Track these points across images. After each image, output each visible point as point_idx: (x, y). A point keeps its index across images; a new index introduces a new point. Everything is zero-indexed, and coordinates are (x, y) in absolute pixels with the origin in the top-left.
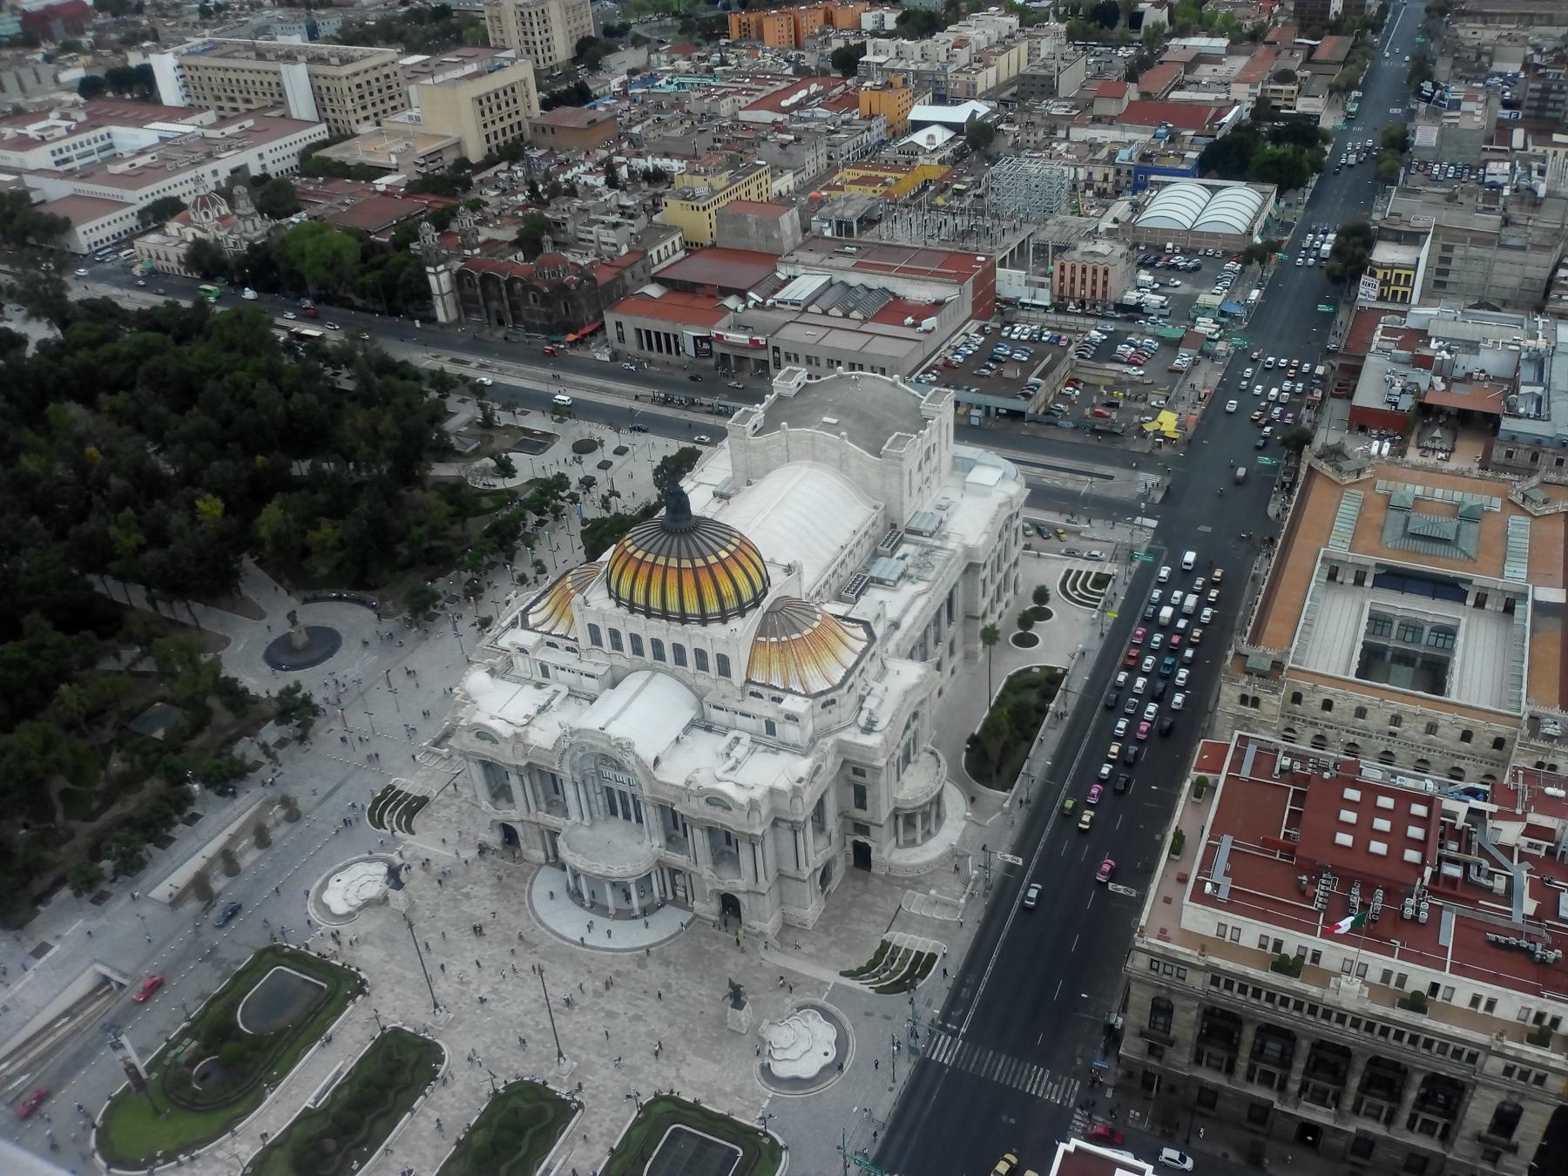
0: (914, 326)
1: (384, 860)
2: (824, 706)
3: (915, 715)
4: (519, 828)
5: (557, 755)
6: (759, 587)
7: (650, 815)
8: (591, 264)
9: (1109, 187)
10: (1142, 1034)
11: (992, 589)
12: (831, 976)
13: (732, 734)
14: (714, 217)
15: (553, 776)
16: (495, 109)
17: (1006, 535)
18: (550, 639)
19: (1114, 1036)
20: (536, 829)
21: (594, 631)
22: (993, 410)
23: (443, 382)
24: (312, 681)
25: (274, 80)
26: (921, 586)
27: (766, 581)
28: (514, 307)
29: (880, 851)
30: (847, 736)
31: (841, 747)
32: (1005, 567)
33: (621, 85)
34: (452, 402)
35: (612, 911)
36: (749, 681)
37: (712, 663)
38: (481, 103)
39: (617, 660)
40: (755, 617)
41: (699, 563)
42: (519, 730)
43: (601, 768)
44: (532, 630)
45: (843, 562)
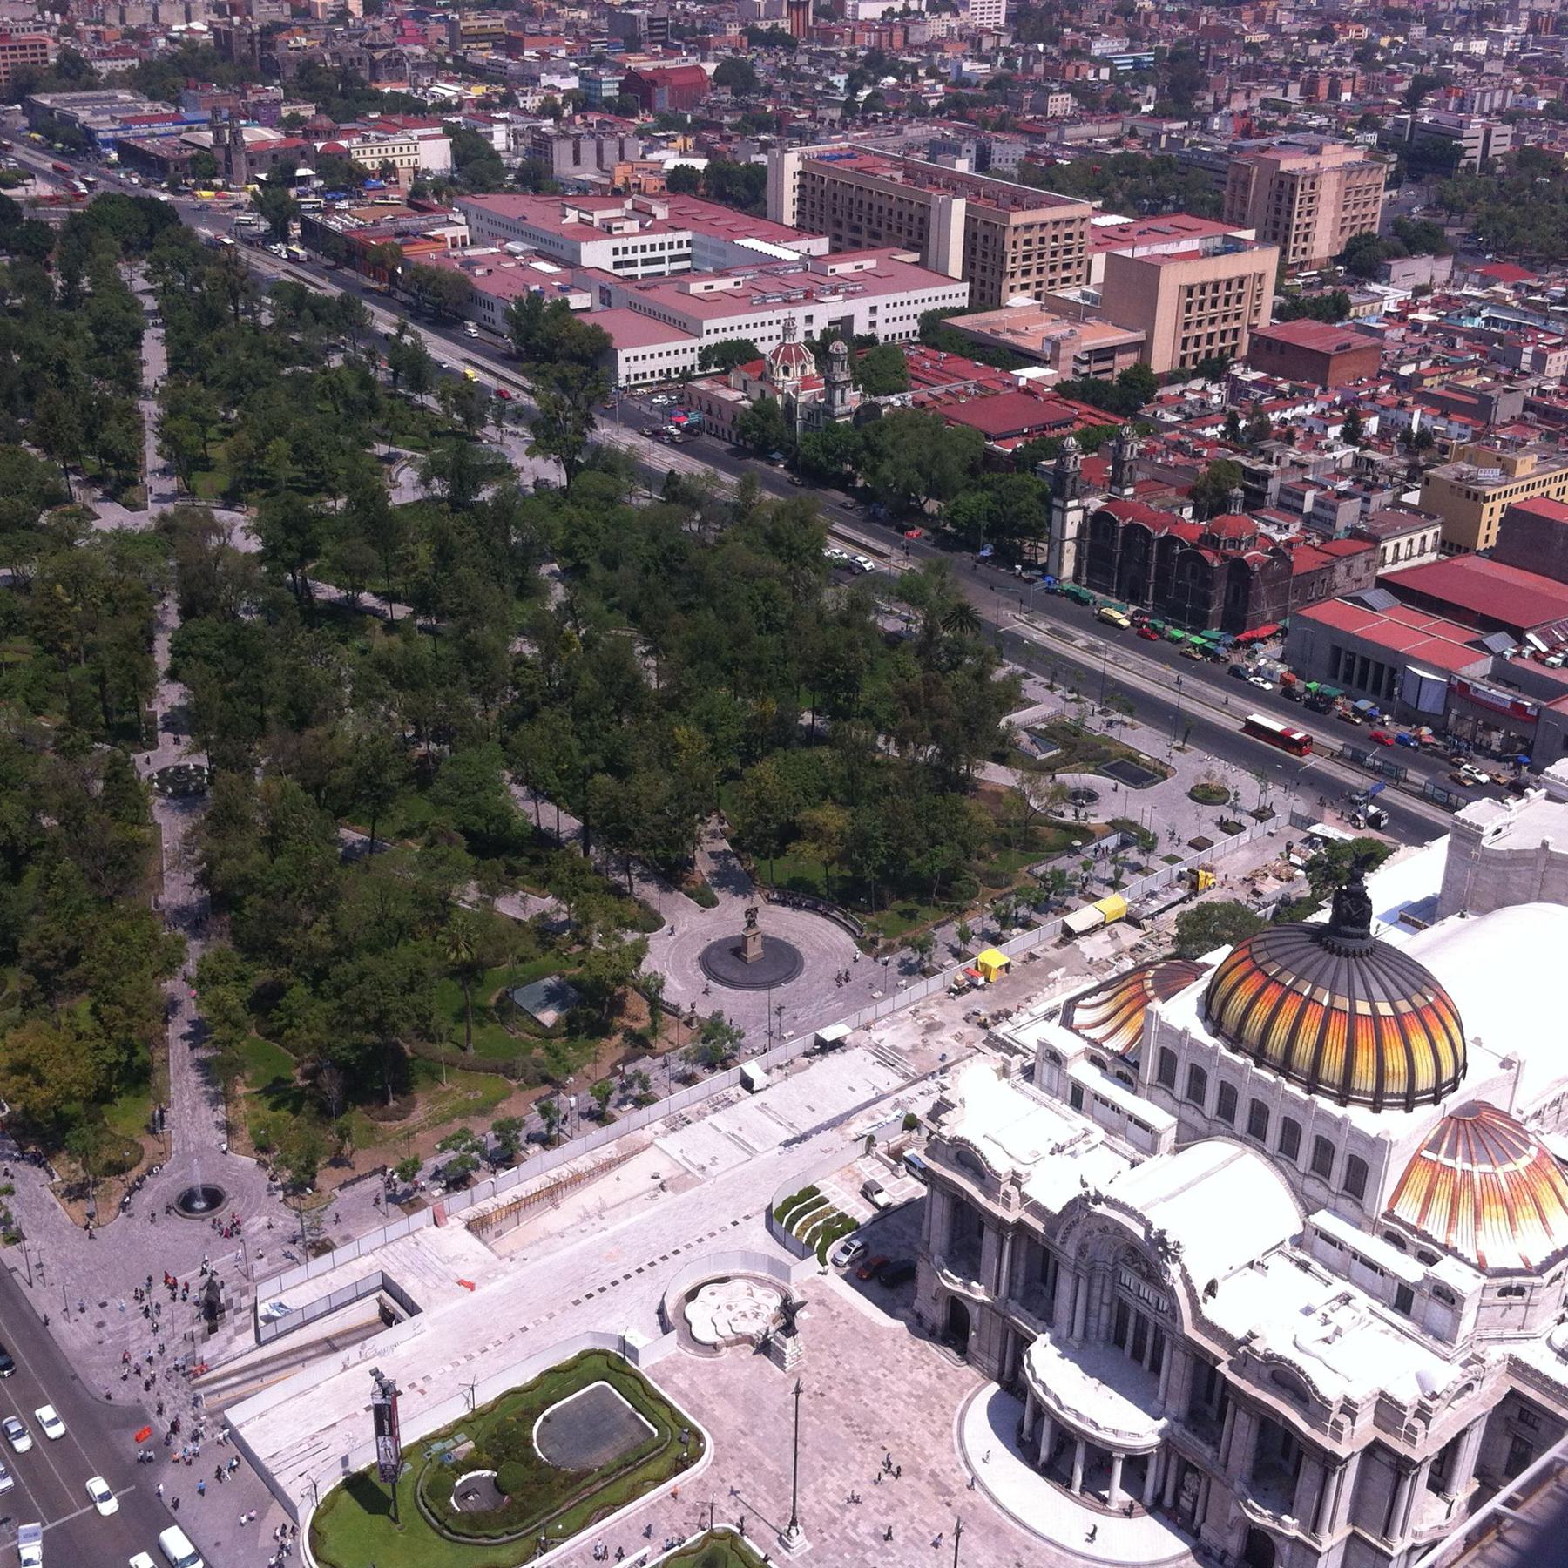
1: (777, 1287)
2: (1505, 1292)
4: (975, 1313)
6: (1448, 1072)
8: (1289, 543)
14: (1498, 515)
20: (998, 1323)
21: (1167, 1061)
27: (1461, 1068)
28: (1162, 576)
31: (1517, 1367)
33: (1400, 304)
34: (1033, 687)
36: (1389, 1215)
37: (1339, 1168)
38: (1190, 294)
39: (1189, 1114)
40: (1427, 1117)
41: (1363, 1008)
42: (1020, 1169)
43: (1122, 1268)
44: (1076, 1031)
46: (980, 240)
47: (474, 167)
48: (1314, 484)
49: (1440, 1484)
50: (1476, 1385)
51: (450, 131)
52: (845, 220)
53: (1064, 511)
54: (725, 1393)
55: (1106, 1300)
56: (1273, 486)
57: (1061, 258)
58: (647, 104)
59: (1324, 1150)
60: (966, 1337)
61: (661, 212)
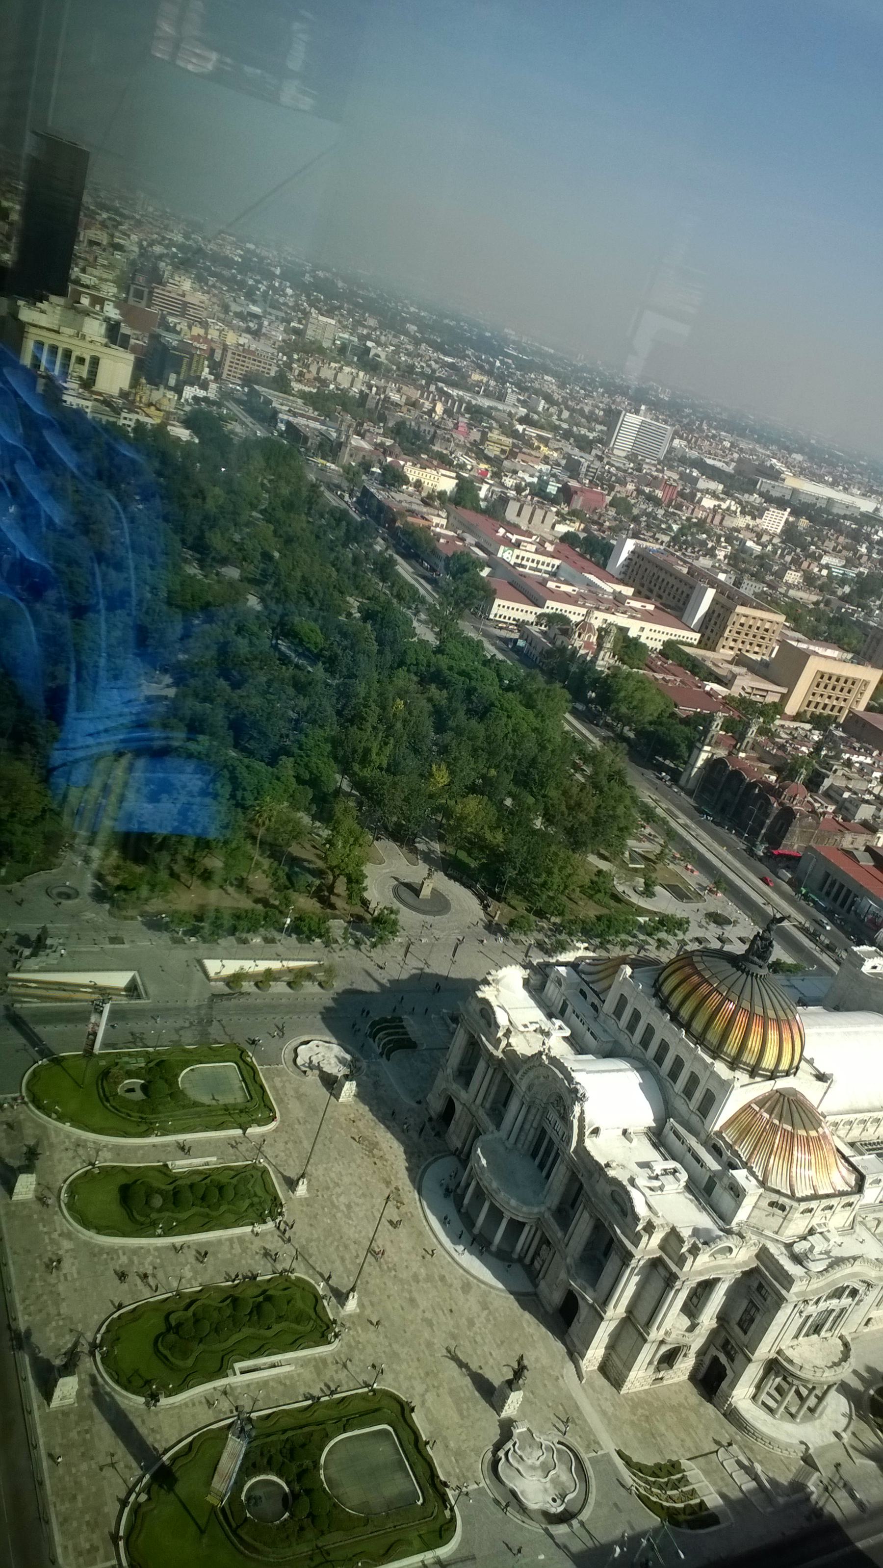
2: (772, 1204)
3: (854, 1293)
4: (458, 1107)
5: (526, 1067)
6: (784, 1065)
7: (559, 1175)
12: (609, 1446)
13: (672, 1164)
15: (512, 1086)
16: (830, 687)
23: (649, 816)
24: (407, 917)
25: (686, 589)
29: (733, 1386)
30: (773, 1249)
31: (763, 1254)
35: (476, 1231)
36: (719, 1134)
37: (698, 1095)
38: (822, 678)
43: (550, 1108)
44: (578, 973)
46: (716, 615)
47: (464, 494)
48: (849, 790)
49: (692, 1309)
50: (735, 1251)
51: (458, 477)
52: (646, 584)
53: (700, 750)
54: (300, 1097)
55: (535, 1125)
56: (827, 783)
57: (758, 640)
58: (568, 502)
59: (694, 1080)
60: (448, 1125)
61: (550, 548)
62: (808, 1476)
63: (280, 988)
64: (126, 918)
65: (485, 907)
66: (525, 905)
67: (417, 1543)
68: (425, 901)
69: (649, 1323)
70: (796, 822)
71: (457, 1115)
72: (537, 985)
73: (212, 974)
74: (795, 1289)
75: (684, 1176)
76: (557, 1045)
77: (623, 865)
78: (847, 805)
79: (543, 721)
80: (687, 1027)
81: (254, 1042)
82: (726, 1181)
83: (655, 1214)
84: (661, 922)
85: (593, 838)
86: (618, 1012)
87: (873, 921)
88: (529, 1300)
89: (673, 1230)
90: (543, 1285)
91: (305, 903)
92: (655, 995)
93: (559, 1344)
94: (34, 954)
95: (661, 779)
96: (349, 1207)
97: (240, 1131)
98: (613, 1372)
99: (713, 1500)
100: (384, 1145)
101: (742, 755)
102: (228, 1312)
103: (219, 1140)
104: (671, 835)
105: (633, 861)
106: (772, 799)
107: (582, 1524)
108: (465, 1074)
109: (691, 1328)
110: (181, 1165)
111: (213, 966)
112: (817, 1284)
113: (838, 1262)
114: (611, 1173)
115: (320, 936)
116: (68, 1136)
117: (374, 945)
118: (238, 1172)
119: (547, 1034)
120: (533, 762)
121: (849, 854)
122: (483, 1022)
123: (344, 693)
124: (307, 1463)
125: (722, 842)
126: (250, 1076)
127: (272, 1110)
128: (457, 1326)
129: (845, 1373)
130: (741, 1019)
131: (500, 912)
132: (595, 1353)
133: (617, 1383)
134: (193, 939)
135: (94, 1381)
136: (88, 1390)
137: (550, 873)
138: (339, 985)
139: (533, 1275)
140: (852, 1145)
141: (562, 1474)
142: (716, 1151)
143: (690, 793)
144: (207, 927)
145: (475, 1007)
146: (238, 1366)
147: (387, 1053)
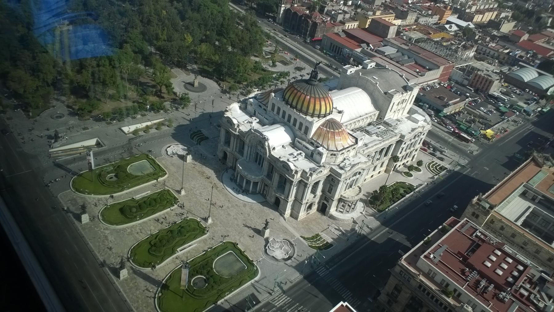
0: (417, 73)
2: (331, 155)
3: (360, 173)
4: (228, 154)
6: (328, 112)
9: (504, 61)
10: (388, 295)
11: (404, 153)
12: (298, 235)
17: (417, 138)
18: (260, 104)
19: (379, 293)
22: (432, 107)
23: (268, 37)
24: (192, 95)
26: (380, 138)
29: (330, 209)
30: (334, 167)
31: (332, 170)
32: (412, 149)
35: (243, 189)
36: (312, 139)
37: (303, 128)
40: (323, 120)
45: (359, 121)
48: (334, 10)
49: (314, 191)
53: (281, 7)
54: (173, 165)
56: (326, 9)
59: (301, 124)
62: (355, 226)
63: (153, 131)
64: (86, 120)
65: (219, 85)
66: (233, 80)
67: (248, 279)
68: (196, 88)
69: (302, 199)
70: (318, 27)
71: (228, 156)
72: (244, 108)
73: (126, 132)
74: (342, 177)
75: (304, 154)
76: (255, 125)
77: (263, 57)
78: (334, 16)
79: (221, 8)
80: (296, 108)
81: (150, 151)
82: (316, 152)
83: (297, 168)
84: (281, 75)
85: (251, 50)
86: (273, 109)
87: (348, 56)
88: (265, 203)
89: (304, 171)
90: (268, 198)
91: (153, 99)
92: (284, 100)
93: (277, 213)
94: (56, 141)
95: (269, 21)
96: (200, 193)
97: (156, 181)
98: (294, 215)
99: (330, 240)
100: (207, 172)
101: (296, 5)
102: (170, 235)
103: (148, 185)
104: (277, 42)
105: (267, 55)
106: (309, 20)
107: (295, 258)
108: (227, 143)
109: (314, 197)
110: (138, 197)
111: (126, 129)
112: (348, 174)
113: (354, 166)
114: (281, 160)
115: (162, 109)
116: (94, 198)
117: (183, 108)
118: (159, 193)
119: (252, 123)
120: (222, 25)
121: (337, 34)
122: (229, 124)
123: (140, 13)
124: (209, 269)
125: (295, 41)
126: (153, 163)
127: (164, 171)
128: (245, 217)
129: (361, 196)
130: (312, 101)
131: (225, 85)
132: (288, 212)
133: (296, 218)
134: (114, 121)
135: (131, 268)
136: (131, 271)
137: (239, 67)
138: (175, 125)
139: (264, 196)
140: (352, 130)
141: (286, 247)
142: (312, 144)
143: (281, 25)
144: (119, 116)
145: (225, 120)
146: (178, 250)
147: (199, 143)
